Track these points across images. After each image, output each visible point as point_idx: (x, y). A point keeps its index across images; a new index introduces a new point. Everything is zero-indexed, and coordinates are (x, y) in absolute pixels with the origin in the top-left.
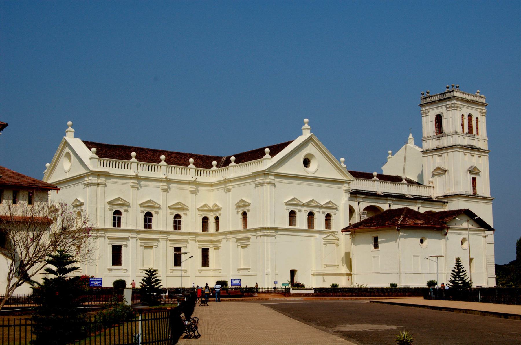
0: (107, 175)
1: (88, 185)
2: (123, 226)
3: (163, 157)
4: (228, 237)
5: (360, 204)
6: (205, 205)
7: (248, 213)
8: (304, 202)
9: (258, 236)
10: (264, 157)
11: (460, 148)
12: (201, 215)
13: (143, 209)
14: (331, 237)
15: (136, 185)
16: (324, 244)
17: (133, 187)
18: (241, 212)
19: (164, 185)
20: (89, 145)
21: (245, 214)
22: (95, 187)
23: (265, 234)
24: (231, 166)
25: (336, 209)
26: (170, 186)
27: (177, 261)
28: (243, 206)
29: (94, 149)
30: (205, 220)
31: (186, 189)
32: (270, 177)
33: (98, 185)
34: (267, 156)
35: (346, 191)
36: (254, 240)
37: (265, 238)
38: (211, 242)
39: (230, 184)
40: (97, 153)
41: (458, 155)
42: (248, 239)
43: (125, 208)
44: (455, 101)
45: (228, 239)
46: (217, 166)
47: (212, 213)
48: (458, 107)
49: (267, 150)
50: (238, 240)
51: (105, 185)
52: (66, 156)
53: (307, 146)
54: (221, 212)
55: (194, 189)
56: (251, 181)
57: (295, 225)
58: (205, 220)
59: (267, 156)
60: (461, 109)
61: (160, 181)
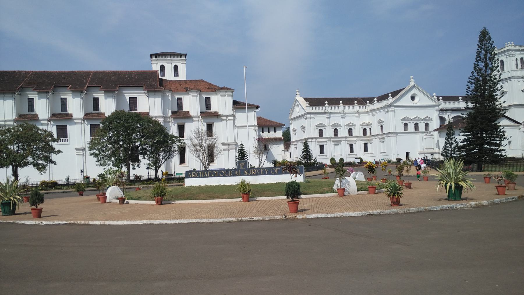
0: (314, 113)
1: (306, 119)
2: (324, 136)
3: (341, 102)
4: (375, 138)
5: (449, 116)
6: (364, 123)
7: (383, 126)
8: (412, 118)
9: (388, 137)
10: (389, 98)
11: (515, 78)
12: (363, 128)
13: (333, 127)
14: (429, 135)
15: (329, 116)
16: (425, 138)
17: (327, 118)
18: (380, 125)
19: (342, 115)
20: (306, 99)
21: (382, 126)
22: (309, 120)
23: (391, 135)
24: (375, 103)
25: (431, 120)
26: (346, 115)
27: (352, 150)
28: (381, 122)
29: (308, 102)
30: (365, 130)
31: (354, 116)
32: (392, 108)
33: (311, 118)
34: (390, 97)
35: (437, 110)
36: (386, 139)
37: (391, 137)
38: (369, 140)
39: (375, 112)
40: (309, 104)
41: (514, 82)
42: (384, 138)
43: (324, 127)
44: (511, 52)
45: (376, 139)
46: (369, 103)
47: (368, 126)
48: (513, 55)
49: (390, 95)
50: (380, 139)
51: (314, 118)
52: (297, 106)
53: (412, 90)
54: (372, 126)
55: (358, 116)
56: (383, 110)
57: (407, 130)
58: (365, 130)
59: (390, 97)
60: (515, 55)
61: (340, 113)
